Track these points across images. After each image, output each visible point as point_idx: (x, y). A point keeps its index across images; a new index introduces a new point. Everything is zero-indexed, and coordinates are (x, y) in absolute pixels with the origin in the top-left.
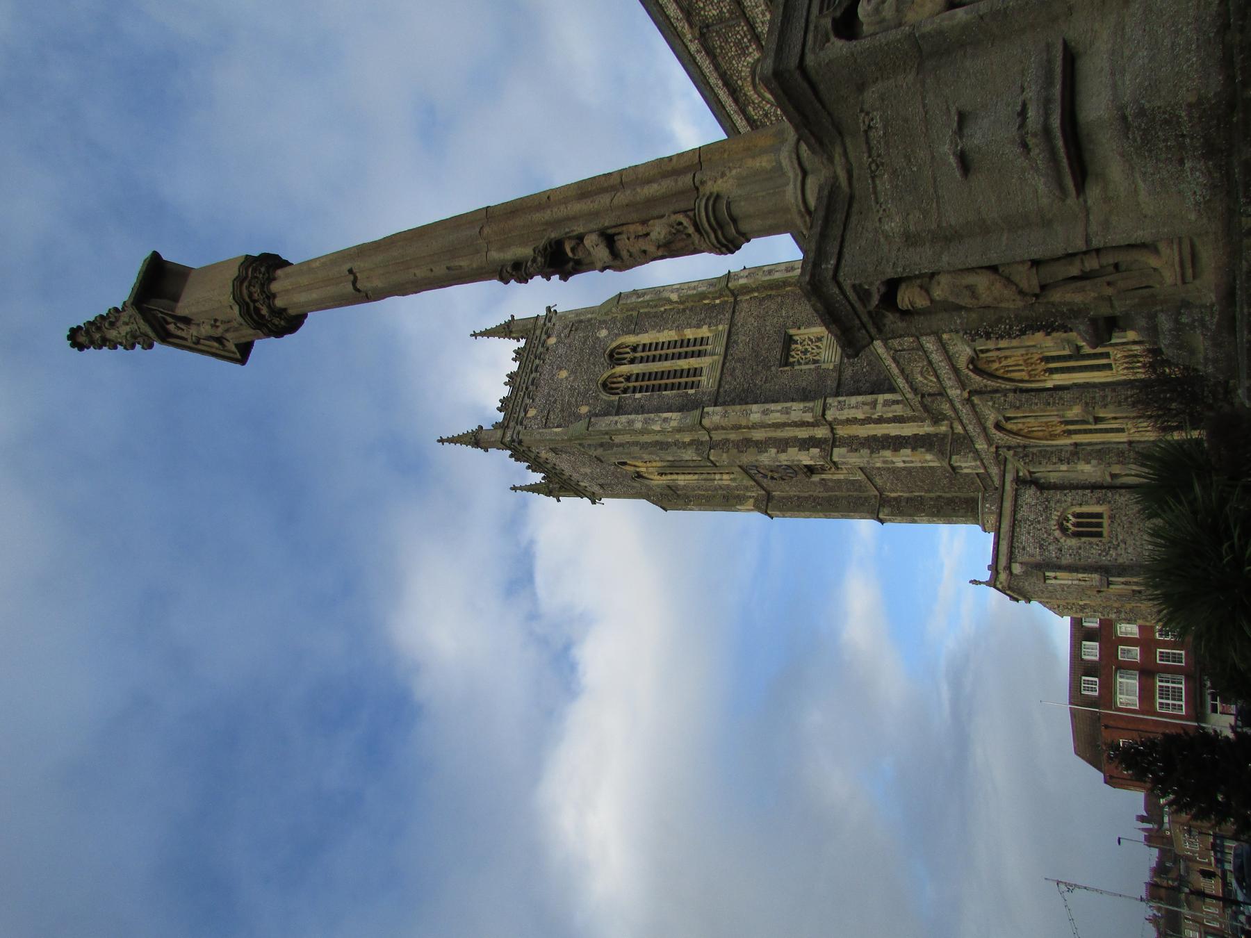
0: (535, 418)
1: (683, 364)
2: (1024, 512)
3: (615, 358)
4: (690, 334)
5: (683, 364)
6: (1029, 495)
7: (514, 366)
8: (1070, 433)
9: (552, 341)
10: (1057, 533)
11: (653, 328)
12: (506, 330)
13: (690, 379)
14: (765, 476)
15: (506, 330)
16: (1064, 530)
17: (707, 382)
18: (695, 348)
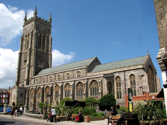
0: (37, 23)
1: (42, 46)
2: (23, 89)
3: (44, 37)
4: (45, 48)
5: (42, 46)
6: (25, 90)
7: (45, 20)
8: (31, 94)
9: (48, 27)
10: (21, 92)
11: (47, 42)
12: (51, 20)
13: (39, 47)
14: (25, 55)
15: (51, 20)
16: (21, 93)
17: (39, 50)
18: (43, 49)
